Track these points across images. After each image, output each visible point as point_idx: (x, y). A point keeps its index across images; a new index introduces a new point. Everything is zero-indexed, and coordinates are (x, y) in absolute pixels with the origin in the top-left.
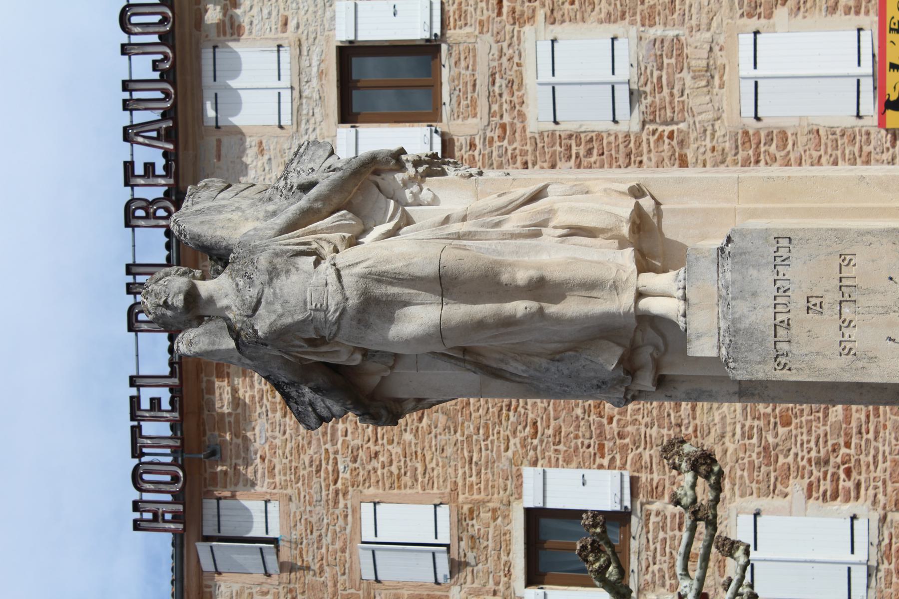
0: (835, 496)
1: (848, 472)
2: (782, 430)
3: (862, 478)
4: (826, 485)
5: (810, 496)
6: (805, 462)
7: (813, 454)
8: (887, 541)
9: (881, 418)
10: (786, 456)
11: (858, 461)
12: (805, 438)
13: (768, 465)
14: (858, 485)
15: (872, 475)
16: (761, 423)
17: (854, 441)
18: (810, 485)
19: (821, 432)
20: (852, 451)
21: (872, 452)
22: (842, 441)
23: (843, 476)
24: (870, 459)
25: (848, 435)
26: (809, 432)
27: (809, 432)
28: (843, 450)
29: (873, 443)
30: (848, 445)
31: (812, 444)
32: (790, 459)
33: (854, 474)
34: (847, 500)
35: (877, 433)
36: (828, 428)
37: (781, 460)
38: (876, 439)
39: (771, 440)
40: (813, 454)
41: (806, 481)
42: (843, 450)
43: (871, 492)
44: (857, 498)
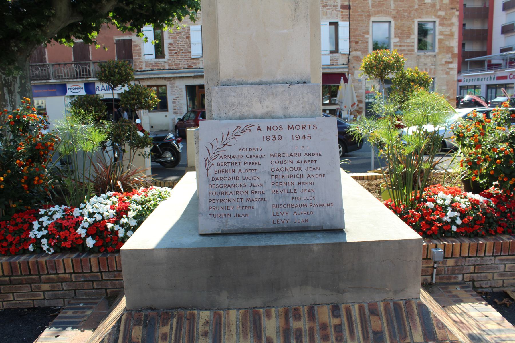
0: (169, 50)
1: (176, 53)
2: (185, 37)
3: (175, 57)
4: (172, 48)
5: (170, 44)
6: (177, 42)
7: (180, 45)
8: (160, 63)
9: (189, 61)
10: (179, 38)
11: (179, 55)
12: (184, 42)
13: (177, 33)
14: (173, 56)
15: (176, 59)
16: (186, 31)
17: (184, 54)
18: (172, 44)
19: (185, 46)
20: (181, 54)
21: (181, 59)
22: (183, 51)
23: (175, 52)
24: (180, 58)
25: (185, 53)
26: (185, 43)
27: (185, 43)
28: (181, 52)
29: (183, 59)
30: (182, 53)
31: (182, 44)
32: (178, 39)
33: (175, 55)
34: (169, 53)
35: (186, 59)
36: (186, 48)
37: (177, 37)
38: (184, 59)
39: (182, 34)
40: (180, 45)
41: (173, 43)
42: (181, 52)
43: (171, 59)
44: (170, 56)
